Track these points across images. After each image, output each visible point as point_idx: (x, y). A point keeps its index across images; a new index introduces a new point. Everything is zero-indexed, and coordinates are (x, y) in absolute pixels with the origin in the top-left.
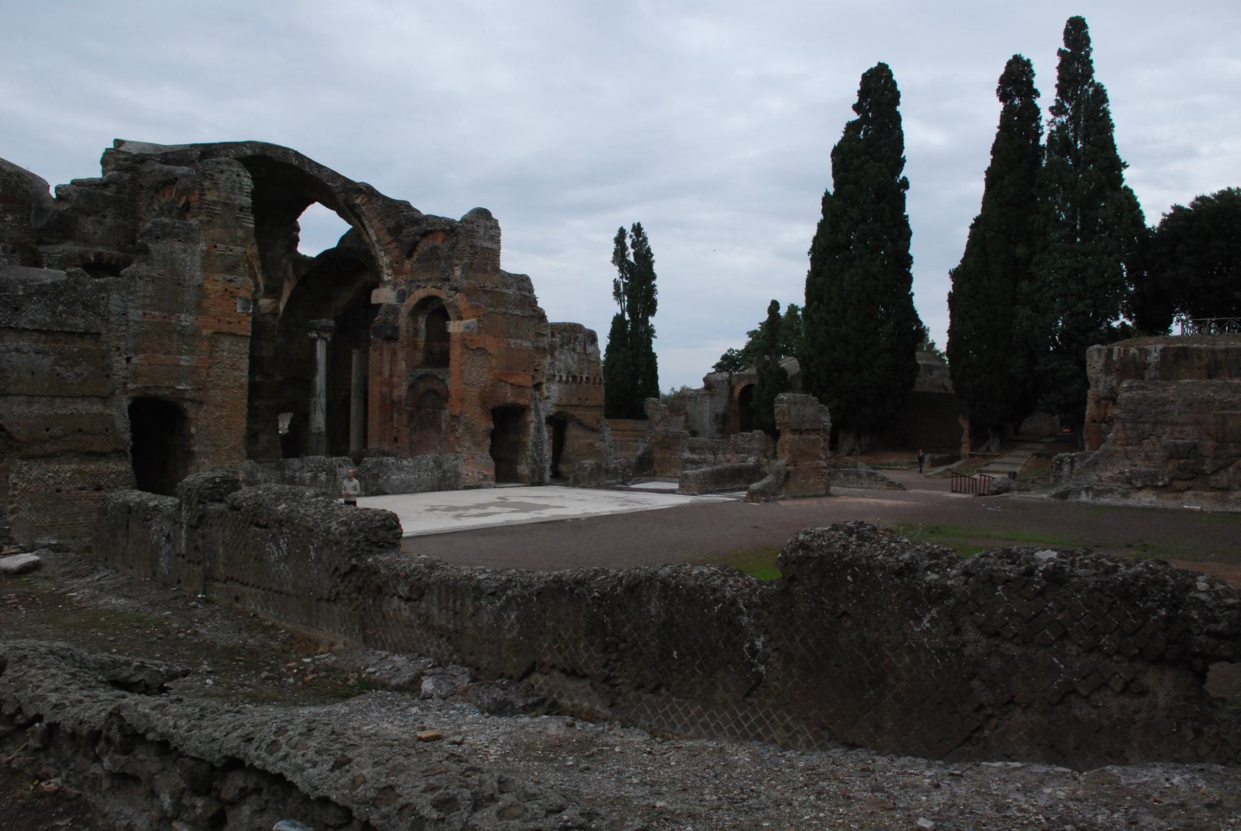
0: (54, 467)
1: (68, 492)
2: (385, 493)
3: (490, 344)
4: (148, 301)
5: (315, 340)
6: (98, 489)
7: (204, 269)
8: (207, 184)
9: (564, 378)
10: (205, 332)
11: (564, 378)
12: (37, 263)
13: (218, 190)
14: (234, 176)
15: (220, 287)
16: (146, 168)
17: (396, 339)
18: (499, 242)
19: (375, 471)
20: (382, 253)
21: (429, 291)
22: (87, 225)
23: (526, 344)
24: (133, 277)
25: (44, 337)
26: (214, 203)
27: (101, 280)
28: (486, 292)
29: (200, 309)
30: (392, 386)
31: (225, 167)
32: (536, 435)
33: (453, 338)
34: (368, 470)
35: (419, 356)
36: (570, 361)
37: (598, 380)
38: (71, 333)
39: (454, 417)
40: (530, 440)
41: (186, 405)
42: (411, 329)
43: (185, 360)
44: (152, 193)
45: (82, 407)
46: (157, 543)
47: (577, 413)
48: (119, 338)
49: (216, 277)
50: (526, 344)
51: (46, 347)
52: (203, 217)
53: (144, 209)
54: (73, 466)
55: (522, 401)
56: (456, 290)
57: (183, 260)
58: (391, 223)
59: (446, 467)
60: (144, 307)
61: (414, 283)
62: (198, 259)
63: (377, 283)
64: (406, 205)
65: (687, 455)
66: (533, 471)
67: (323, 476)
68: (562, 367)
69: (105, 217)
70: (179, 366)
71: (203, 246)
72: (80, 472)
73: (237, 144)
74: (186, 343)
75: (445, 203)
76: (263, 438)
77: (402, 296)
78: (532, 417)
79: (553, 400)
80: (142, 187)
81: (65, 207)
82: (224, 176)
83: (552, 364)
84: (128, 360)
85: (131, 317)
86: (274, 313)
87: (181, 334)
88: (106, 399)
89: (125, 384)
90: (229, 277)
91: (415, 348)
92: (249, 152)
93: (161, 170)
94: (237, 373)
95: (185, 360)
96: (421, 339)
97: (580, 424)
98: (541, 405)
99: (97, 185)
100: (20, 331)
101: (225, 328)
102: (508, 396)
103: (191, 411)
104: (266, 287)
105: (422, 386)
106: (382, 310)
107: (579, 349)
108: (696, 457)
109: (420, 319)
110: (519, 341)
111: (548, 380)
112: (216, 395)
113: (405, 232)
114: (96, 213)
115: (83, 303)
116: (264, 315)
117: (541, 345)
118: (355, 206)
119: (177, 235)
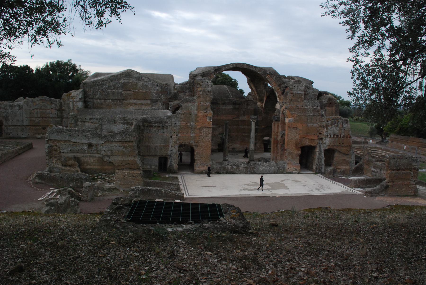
2: (256, 173)
3: (299, 126)
4: (182, 120)
5: (251, 122)
6: (134, 177)
7: (197, 110)
10: (198, 127)
11: (332, 136)
14: (206, 83)
15: (202, 114)
19: (253, 166)
22: (181, 95)
26: (200, 91)
28: (298, 108)
29: (196, 121)
30: (277, 136)
32: (319, 156)
36: (335, 130)
37: (349, 137)
43: (192, 135)
45: (129, 158)
47: (338, 148)
48: (174, 130)
50: (316, 125)
58: (279, 83)
59: (280, 166)
60: (181, 121)
62: (196, 107)
65: (373, 169)
67: (235, 167)
68: (331, 132)
70: (190, 136)
71: (197, 104)
72: (129, 173)
73: (228, 65)
78: (317, 150)
79: (327, 144)
81: (176, 91)
84: (177, 135)
85: (177, 124)
86: (262, 107)
87: (191, 128)
90: (205, 111)
92: (232, 67)
97: (339, 152)
98: (322, 146)
101: (204, 125)
102: (307, 143)
103: (195, 148)
107: (339, 126)
108: (375, 170)
110: (312, 124)
114: (184, 92)
116: (259, 108)
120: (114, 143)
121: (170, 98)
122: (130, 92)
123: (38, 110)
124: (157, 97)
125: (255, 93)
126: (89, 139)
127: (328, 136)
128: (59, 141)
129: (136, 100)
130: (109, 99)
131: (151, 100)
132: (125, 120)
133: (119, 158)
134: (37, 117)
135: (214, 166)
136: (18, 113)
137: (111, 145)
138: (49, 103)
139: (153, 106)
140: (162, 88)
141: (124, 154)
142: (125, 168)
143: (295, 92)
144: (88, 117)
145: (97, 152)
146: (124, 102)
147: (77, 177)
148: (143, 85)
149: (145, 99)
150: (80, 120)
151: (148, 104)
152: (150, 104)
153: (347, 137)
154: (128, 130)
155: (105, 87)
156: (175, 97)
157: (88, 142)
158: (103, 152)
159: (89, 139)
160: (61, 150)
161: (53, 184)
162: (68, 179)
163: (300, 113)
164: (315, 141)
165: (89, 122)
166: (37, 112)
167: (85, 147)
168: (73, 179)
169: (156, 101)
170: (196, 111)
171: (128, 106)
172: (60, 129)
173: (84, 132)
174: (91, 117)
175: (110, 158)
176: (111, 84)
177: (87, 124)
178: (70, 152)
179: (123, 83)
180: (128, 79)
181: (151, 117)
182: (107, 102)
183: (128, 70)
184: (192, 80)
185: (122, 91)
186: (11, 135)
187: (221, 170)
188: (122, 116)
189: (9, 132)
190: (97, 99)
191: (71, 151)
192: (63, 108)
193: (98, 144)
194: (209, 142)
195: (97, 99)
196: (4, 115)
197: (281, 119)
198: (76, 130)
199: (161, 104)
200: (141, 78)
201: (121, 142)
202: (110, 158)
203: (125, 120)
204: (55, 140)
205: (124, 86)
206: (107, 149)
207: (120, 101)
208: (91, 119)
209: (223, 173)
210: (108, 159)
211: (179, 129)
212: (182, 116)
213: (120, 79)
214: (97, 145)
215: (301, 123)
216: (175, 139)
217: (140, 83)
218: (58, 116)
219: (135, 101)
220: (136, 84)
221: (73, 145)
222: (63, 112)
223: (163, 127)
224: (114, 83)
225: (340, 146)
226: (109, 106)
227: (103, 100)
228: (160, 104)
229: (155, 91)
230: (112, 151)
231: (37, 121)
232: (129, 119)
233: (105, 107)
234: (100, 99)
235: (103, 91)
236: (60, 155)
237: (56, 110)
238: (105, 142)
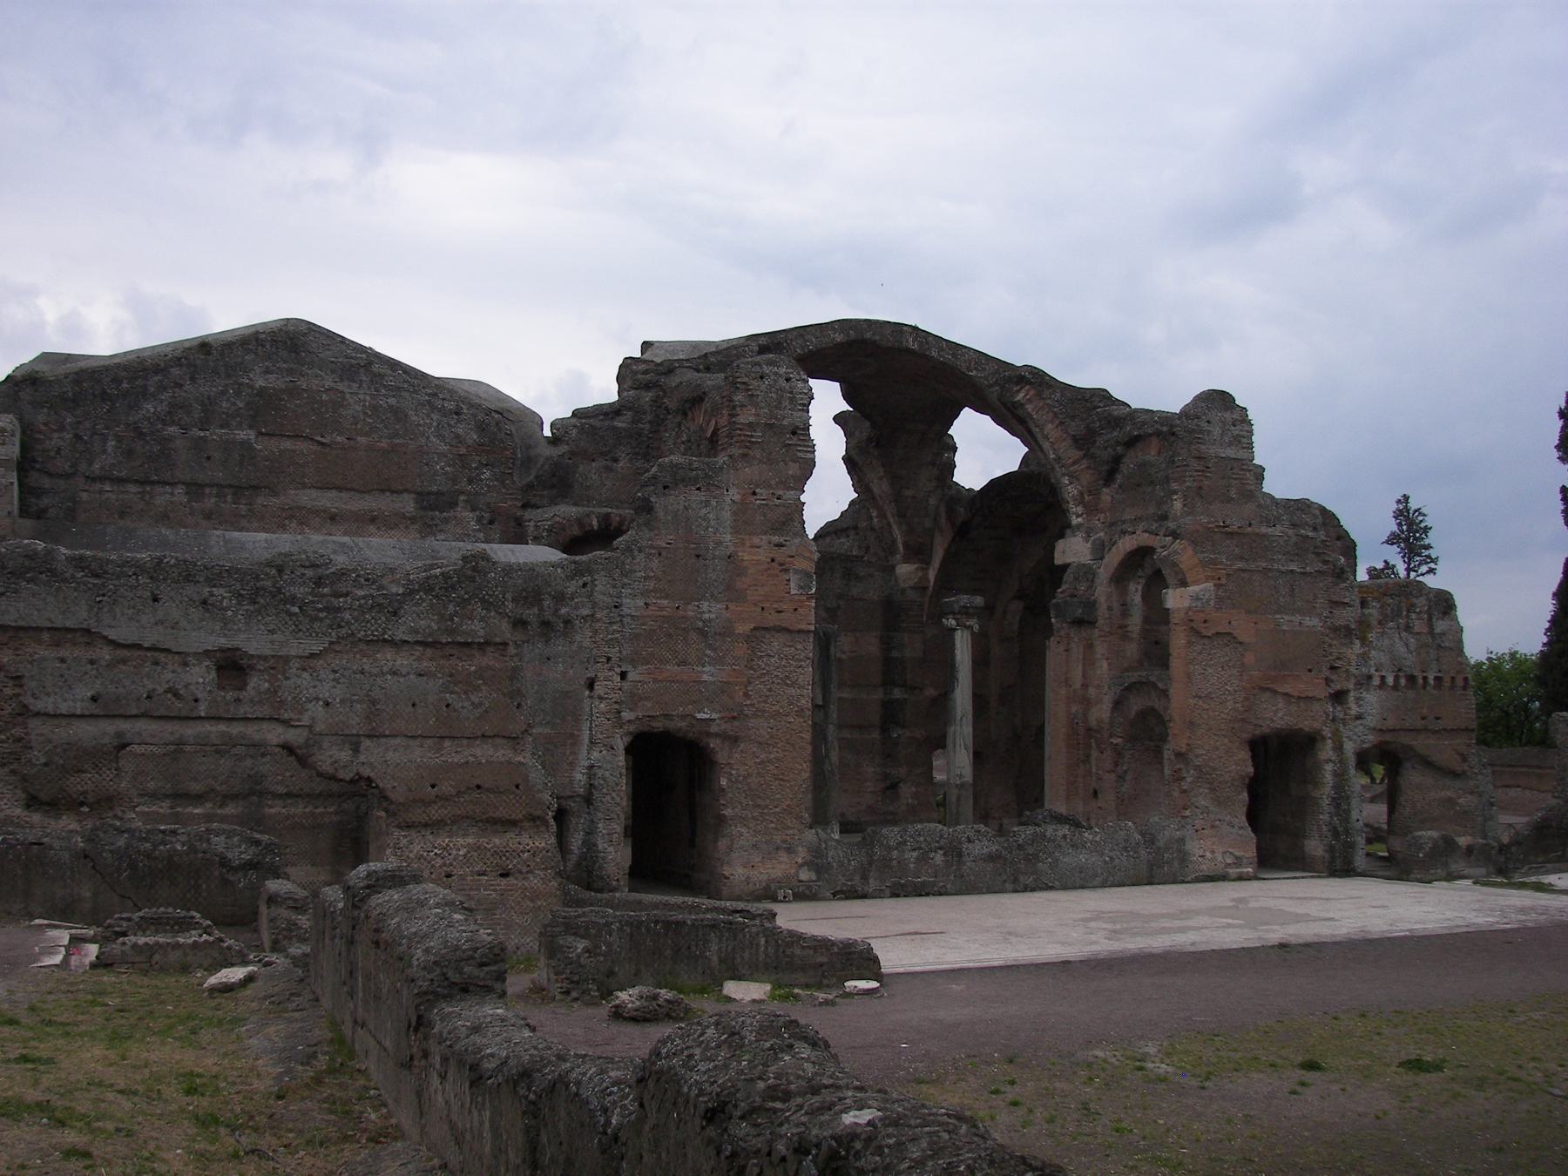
0: (443, 840)
1: (462, 877)
4: (652, 585)
6: (504, 875)
7: (736, 530)
8: (739, 397)
9: (1390, 680)
10: (742, 628)
11: (1390, 680)
12: (520, 539)
13: (756, 405)
14: (782, 382)
15: (762, 556)
16: (674, 381)
17: (1092, 623)
18: (1250, 446)
20: (1066, 480)
21: (1142, 539)
22: (591, 472)
23: (1312, 622)
25: (429, 652)
27: (584, 558)
30: (1086, 702)
31: (766, 369)
33: (1175, 618)
34: (1020, 847)
35: (1132, 650)
37: (1460, 682)
39: (1179, 755)
40: (1325, 793)
41: (713, 743)
42: (1115, 605)
43: (708, 674)
44: (678, 419)
45: (483, 752)
47: (1420, 743)
49: (756, 540)
50: (1312, 622)
54: (470, 840)
55: (1306, 725)
56: (1175, 535)
60: (645, 593)
61: (1116, 528)
62: (727, 515)
63: (1063, 529)
64: (1102, 395)
66: (1331, 849)
67: (939, 858)
69: (616, 460)
71: (734, 494)
74: (710, 647)
75: (1156, 384)
76: (907, 791)
77: (1100, 551)
78: (1326, 752)
79: (1371, 721)
83: (1364, 657)
84: (623, 675)
85: (626, 611)
86: (921, 588)
87: (702, 633)
88: (514, 740)
89: (619, 712)
90: (776, 539)
91: (1125, 637)
92: (839, 338)
95: (708, 674)
96: (1135, 622)
97: (1427, 763)
99: (606, 414)
101: (772, 619)
104: (906, 545)
105: (1136, 704)
106: (1068, 576)
107: (1419, 626)
109: (1132, 587)
111: (1359, 684)
113: (1100, 441)
115: (483, 600)
117: (1341, 622)
120: (389, 654)
121: (530, 486)
122: (302, 446)
124: (455, 481)
125: (882, 515)
126: (225, 622)
127: (1370, 677)
129: (334, 493)
130: (172, 484)
131: (421, 495)
133: (419, 754)
137: (367, 664)
139: (429, 529)
140: (481, 428)
142: (456, 820)
143: (1213, 451)
147: (193, 849)
148: (375, 408)
149: (386, 489)
151: (404, 516)
152: (413, 520)
153: (1453, 687)
155: (149, 407)
157: (223, 642)
158: (317, 710)
160: (29, 700)
163: (1242, 558)
164: (1316, 706)
167: (200, 676)
169: (453, 504)
170: (728, 537)
172: (32, 556)
175: (356, 750)
179: (262, 392)
180: (290, 372)
182: (158, 501)
185: (252, 434)
190: (91, 479)
191: (102, 707)
193: (286, 660)
195: (91, 479)
197: (1102, 610)
198: (139, 568)
199: (479, 520)
201: (434, 644)
202: (356, 750)
205: (265, 410)
209: (878, 895)
210: (345, 755)
211: (637, 636)
212: (655, 563)
214: (278, 664)
215: (1248, 612)
216: (615, 696)
219: (328, 500)
223: (546, 624)
225: (1426, 729)
227: (133, 488)
228: (469, 516)
229: (443, 448)
230: (374, 702)
234: (121, 481)
235: (141, 435)
236: (18, 731)
238: (330, 649)
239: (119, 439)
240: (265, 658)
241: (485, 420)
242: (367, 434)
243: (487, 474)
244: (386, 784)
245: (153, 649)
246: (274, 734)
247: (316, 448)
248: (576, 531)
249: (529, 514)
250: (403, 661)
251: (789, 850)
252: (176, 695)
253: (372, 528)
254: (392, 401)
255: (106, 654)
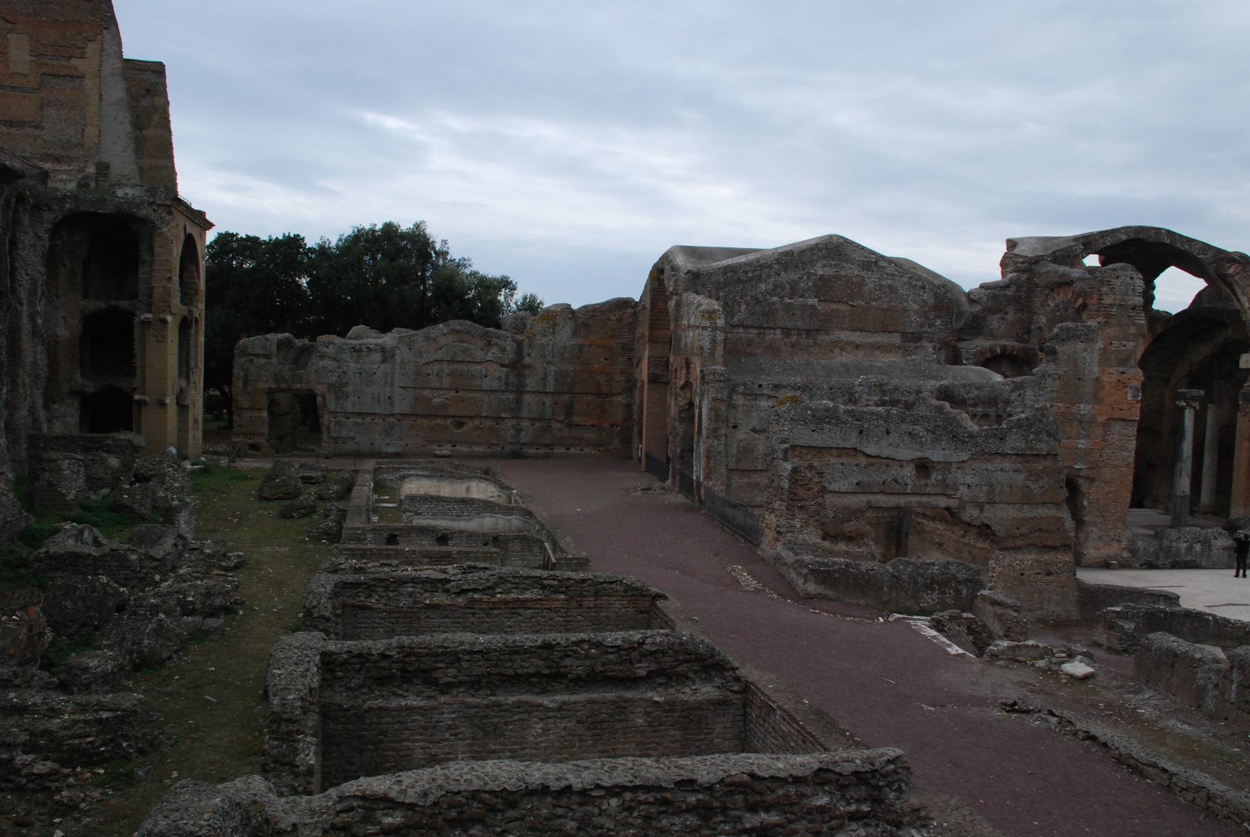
0: (1020, 556)
4: (1054, 395)
5: (1183, 409)
7: (1100, 364)
8: (1105, 289)
10: (1101, 419)
13: (1114, 294)
15: (1114, 378)
22: (994, 322)
24: (1043, 376)
29: (1096, 399)
31: (1120, 273)
38: (1038, 455)
41: (1081, 481)
43: (1082, 444)
45: (1042, 512)
46: (1205, 687)
49: (1111, 370)
51: (1020, 467)
52: (1100, 319)
53: (1038, 305)
57: (1084, 358)
60: (1052, 400)
62: (1096, 356)
67: (1198, 547)
71: (1100, 345)
73: (1113, 231)
80: (1037, 285)
81: (977, 308)
82: (1119, 282)
87: (1080, 422)
90: (1121, 369)
92: (1124, 237)
93: (1056, 272)
94: (1126, 454)
100: (1004, 455)
101: (1118, 414)
103: (1084, 485)
112: (1107, 473)
114: (1000, 311)
118: (1226, 275)
119: (1079, 337)
120: (999, 459)
122: (842, 307)
123: (447, 368)
124: (922, 326)
126: (921, 443)
128: (820, 450)
129: (858, 333)
131: (904, 334)
132: (884, 395)
134: (440, 389)
135: (1140, 544)
136: (379, 373)
138: (481, 343)
139: (908, 352)
140: (936, 296)
141: (1027, 500)
142: (1028, 546)
144: (765, 381)
145: (946, 489)
146: (821, 337)
147: (942, 573)
148: (881, 286)
149: (885, 331)
150: (741, 389)
152: (899, 348)
154: (1042, 415)
155: (763, 286)
156: (975, 327)
157: (919, 454)
158: (963, 490)
159: (921, 443)
160: (827, 485)
161: (862, 602)
162: (916, 582)
165: (770, 397)
166: (442, 370)
167: (908, 472)
168: (933, 581)
171: (832, 351)
172: (827, 410)
173: (903, 420)
174: (775, 380)
175: (982, 511)
176: (785, 277)
177: (764, 403)
178: (858, 489)
180: (836, 266)
181: (964, 386)
182: (767, 338)
183: (831, 237)
184: (1024, 277)
186: (350, 446)
187: (1158, 557)
188: (873, 379)
189: (344, 433)
191: (862, 488)
192: (527, 360)
193: (951, 463)
194: (1127, 466)
196: (334, 379)
199: (934, 348)
200: (876, 263)
202: (982, 511)
203: (884, 393)
204: (809, 447)
205: (823, 287)
206: (976, 480)
207: (808, 337)
208: (777, 387)
210: (976, 513)
213: (812, 263)
214: (947, 465)
217: (872, 279)
218: (507, 384)
219: (856, 337)
220: (862, 283)
221: (866, 467)
222: (526, 372)
223: (999, 416)
224: (793, 275)
226: (773, 349)
227: (755, 331)
229: (916, 307)
230: (992, 485)
231: (437, 400)
232: (896, 389)
233: (759, 351)
235: (759, 302)
236: (820, 500)
237: (503, 366)
239: (748, 305)
240: (940, 463)
241: (939, 294)
242: (876, 300)
243: (939, 322)
244: (995, 528)
245: (887, 458)
246: (943, 502)
247: (849, 308)
248: (988, 355)
249: (960, 345)
250: (1007, 465)
251: (1119, 541)
252: (897, 482)
253: (877, 352)
254: (889, 282)
255: (863, 461)
